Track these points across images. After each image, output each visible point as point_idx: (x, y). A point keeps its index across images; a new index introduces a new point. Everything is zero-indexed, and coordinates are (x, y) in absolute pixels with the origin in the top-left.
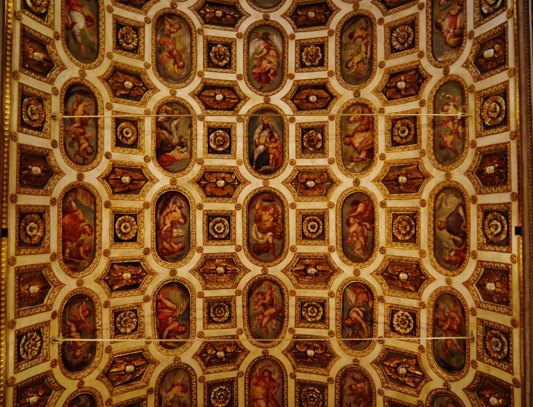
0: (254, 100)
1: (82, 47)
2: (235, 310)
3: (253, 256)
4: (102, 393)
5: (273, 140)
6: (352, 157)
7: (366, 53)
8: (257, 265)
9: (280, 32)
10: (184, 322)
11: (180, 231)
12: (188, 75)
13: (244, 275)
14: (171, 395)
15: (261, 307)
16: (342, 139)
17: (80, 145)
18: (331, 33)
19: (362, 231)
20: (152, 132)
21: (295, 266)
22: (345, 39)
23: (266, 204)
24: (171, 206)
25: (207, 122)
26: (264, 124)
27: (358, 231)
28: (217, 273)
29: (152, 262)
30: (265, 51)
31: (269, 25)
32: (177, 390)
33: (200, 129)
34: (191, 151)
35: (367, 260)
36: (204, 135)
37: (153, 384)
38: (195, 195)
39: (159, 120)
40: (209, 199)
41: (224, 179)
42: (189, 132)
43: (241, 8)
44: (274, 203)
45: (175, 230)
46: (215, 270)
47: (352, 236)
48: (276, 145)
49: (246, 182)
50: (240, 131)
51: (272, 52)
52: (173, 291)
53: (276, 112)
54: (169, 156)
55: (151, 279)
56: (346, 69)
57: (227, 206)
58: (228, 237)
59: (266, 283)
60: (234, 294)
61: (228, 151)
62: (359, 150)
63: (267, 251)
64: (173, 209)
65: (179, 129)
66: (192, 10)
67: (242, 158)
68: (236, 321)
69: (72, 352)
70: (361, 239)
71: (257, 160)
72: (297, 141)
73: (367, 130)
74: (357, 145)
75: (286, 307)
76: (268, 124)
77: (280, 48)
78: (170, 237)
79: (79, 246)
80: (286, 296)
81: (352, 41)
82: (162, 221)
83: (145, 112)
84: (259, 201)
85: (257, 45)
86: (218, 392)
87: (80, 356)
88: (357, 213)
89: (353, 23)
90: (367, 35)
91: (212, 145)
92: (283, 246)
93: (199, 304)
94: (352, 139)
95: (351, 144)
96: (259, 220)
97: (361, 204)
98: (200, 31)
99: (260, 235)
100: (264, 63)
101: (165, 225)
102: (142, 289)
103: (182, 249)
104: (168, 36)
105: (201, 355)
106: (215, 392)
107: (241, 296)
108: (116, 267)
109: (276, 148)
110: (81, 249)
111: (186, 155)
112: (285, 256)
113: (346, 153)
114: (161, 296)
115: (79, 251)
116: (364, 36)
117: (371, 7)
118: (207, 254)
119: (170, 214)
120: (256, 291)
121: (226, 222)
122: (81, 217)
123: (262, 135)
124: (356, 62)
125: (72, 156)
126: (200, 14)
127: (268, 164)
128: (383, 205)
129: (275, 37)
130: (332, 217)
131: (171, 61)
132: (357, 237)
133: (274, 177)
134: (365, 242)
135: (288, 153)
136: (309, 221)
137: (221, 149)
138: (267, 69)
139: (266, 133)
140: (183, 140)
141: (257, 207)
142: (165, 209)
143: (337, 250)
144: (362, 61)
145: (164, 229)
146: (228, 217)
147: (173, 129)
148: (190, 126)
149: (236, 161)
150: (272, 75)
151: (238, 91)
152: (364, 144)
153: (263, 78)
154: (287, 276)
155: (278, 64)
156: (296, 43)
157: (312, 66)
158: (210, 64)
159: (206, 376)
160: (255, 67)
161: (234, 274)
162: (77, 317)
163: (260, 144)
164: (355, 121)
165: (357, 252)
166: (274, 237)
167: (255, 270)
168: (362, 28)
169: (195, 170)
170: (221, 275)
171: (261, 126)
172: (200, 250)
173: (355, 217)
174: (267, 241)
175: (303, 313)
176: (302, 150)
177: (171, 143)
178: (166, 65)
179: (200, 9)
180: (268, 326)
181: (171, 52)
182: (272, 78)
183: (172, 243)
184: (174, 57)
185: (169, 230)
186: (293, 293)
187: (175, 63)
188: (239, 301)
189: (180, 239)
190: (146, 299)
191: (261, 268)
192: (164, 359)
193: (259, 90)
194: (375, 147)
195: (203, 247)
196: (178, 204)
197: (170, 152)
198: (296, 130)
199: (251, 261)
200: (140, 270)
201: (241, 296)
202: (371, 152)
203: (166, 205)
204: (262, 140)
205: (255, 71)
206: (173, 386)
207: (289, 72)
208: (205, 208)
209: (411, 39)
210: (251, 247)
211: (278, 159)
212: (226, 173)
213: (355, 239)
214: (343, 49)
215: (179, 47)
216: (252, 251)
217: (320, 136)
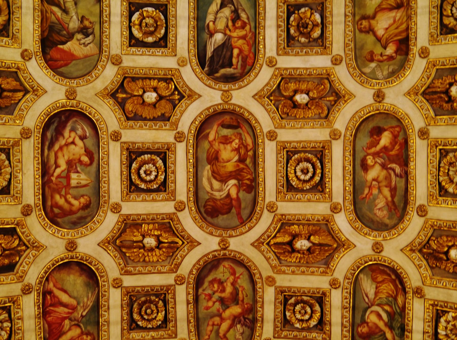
2: (175, 308)
3: (204, 219)
5: (239, 24)
6: (372, 53)
8: (211, 234)
10: (89, 328)
11: (83, 176)
13: (189, 251)
15: (217, 304)
16: (355, 23)
19: (388, 178)
20: (34, 9)
21: (275, 237)
23: (226, 132)
24: (66, 133)
27: (381, 178)
28: (144, 247)
29: (37, 228)
35: (395, 226)
36: (122, 15)
38: (108, 116)
40: (131, 123)
41: (155, 90)
42: (96, 9)
44: (240, 130)
45: (74, 176)
46: (141, 241)
47: (370, 187)
48: (242, 33)
49: (193, 96)
52: (72, 277)
54: (63, 51)
55: (35, 257)
58: (163, 187)
59: (226, 264)
60: (173, 282)
61: (163, 43)
63: (228, 211)
64: (71, 140)
67: (186, 55)
68: (175, 326)
70: (386, 192)
71: (212, 57)
72: (279, 26)
73: (398, 7)
74: (380, 32)
75: (259, 305)
80: (259, 285)
84: (215, 127)
88: (378, 148)
91: (136, 33)
92: (255, 202)
93: (115, 298)
94: (373, 22)
95: (371, 30)
96: (214, 159)
99: (216, 184)
101: (57, 166)
102: (20, 273)
103: (86, 207)
107: (184, 286)
109: (244, 37)
111: (92, 49)
112: (258, 220)
113: (362, 48)
114: (51, 285)
118: (128, 216)
119: (65, 149)
120: (210, 278)
121: (160, 163)
123: (219, 15)
127: (230, 65)
128: (423, 134)
130: (338, 154)
132: (379, 188)
133: (240, 88)
134: (393, 196)
136: (299, 161)
137: (150, 39)
139: (227, 12)
140: (87, 23)
141: (211, 137)
142: (57, 139)
146: (163, 153)
149: (175, 59)
152: (392, 31)
154: (262, 252)
161: (173, 248)
163: (217, 31)
165: (379, 213)
166: (239, 187)
167: (208, 243)
169: (108, 75)
170: (151, 250)
172: (116, 208)
174: (228, 195)
175: (288, 314)
176: (288, 42)
177: (67, 29)
180: (228, 335)
183: (69, 196)
185: (64, 174)
186: (271, 281)
188: (182, 294)
189: (82, 191)
190: (27, 290)
191: (218, 239)
194: (412, 36)
195: (121, 204)
196: (80, 132)
197: (64, 43)
199: (201, 227)
200: (17, 242)
201: (184, 286)
202: (404, 44)
203: (59, 133)
204: (221, 25)
208: (123, 139)
211: (247, 56)
212: (160, 80)
213: (375, 191)
216: (202, 210)
217: (317, 17)
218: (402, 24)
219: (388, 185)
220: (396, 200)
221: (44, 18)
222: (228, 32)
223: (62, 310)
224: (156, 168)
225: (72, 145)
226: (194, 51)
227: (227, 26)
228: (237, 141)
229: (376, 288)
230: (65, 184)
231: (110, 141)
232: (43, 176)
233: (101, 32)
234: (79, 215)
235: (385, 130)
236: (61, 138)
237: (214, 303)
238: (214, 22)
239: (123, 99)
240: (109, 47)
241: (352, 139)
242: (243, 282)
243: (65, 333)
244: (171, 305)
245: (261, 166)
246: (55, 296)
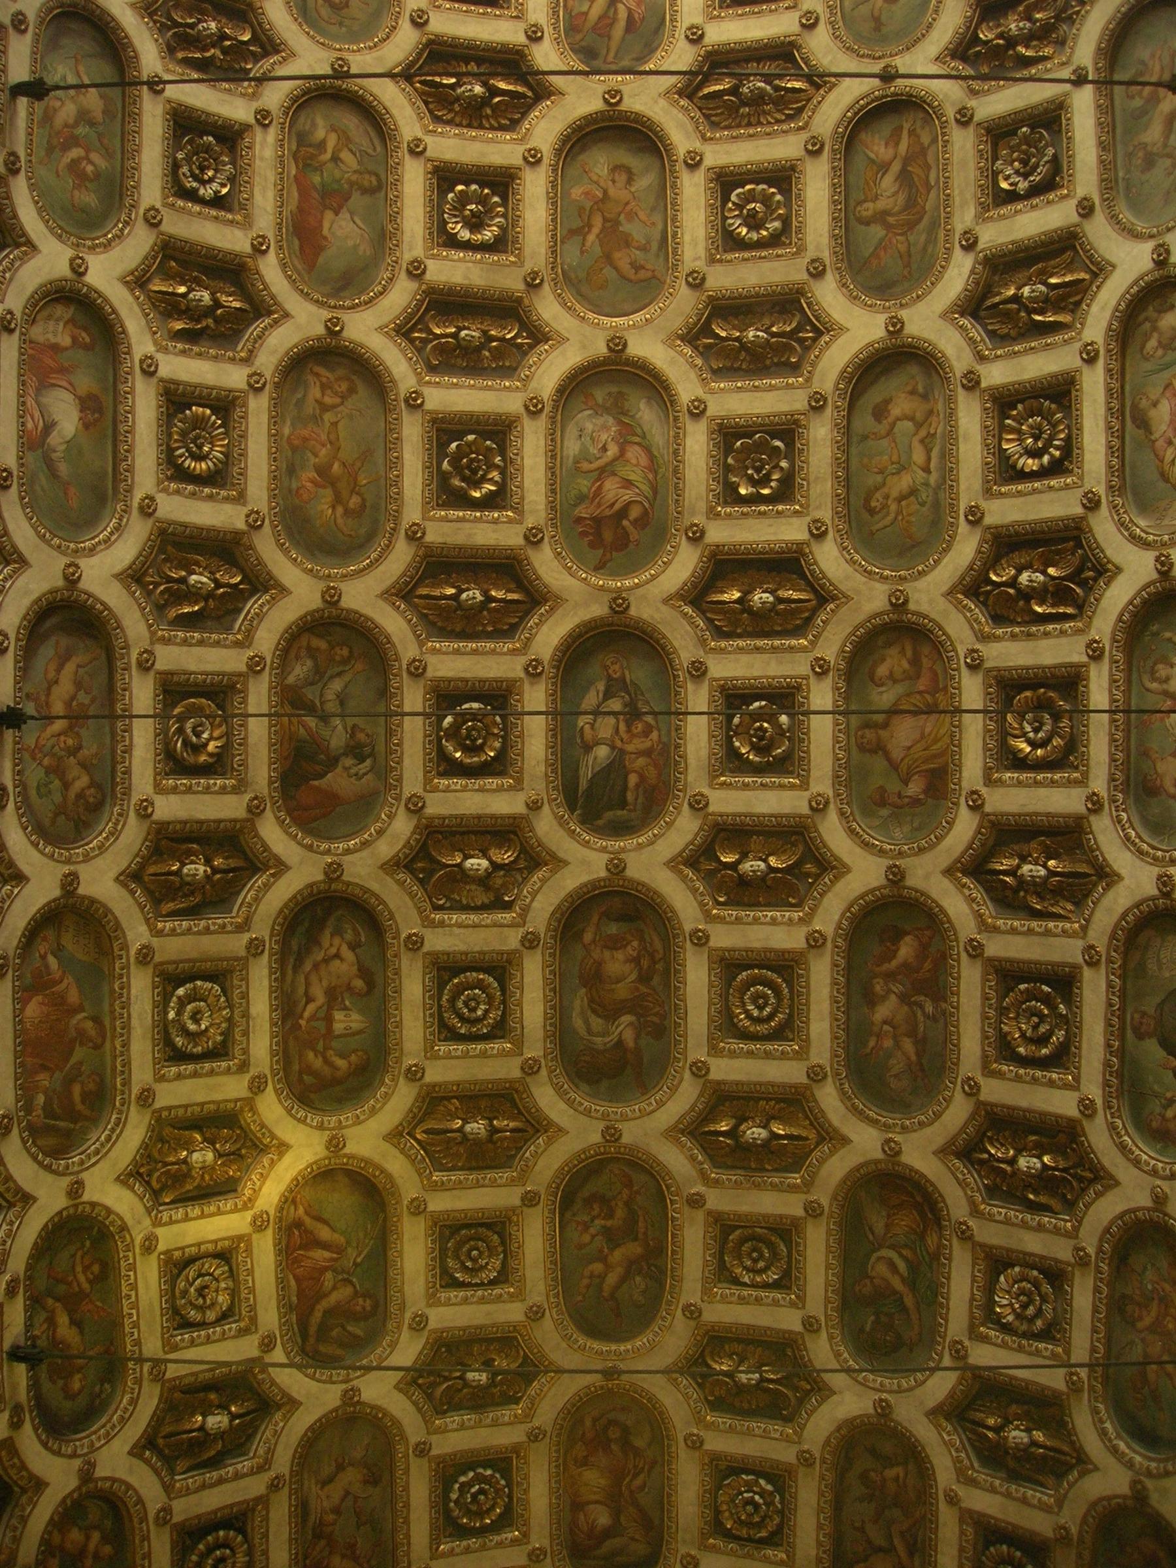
1: (72, 490)
4: (142, 1491)
5: (639, 727)
7: (927, 470)
11: (355, 1016)
14: (335, 1492)
17: (66, 786)
23: (613, 929)
24: (326, 942)
26: (610, 678)
32: (351, 1477)
37: (283, 1462)
38: (400, 902)
39: (291, 680)
45: (338, 1015)
47: (879, 1036)
54: (318, 789)
56: (866, 516)
58: (500, 1030)
60: (518, 1202)
64: (333, 951)
69: (61, 1383)
70: (908, 1045)
71: (590, 788)
74: (897, 754)
79: (69, 1082)
82: (301, 990)
84: (595, 918)
86: (469, 1484)
87: (80, 1391)
94: (883, 734)
95: (879, 748)
96: (594, 978)
97: (908, 939)
99: (597, 1023)
101: (309, 1000)
105: (417, 1380)
106: (462, 1485)
108: (167, 1131)
109: (648, 753)
110: (77, 1090)
116: (919, 416)
119: (323, 966)
124: (894, 493)
126: (412, 341)
127: (623, 804)
129: (642, 405)
131: (327, 494)
132: (895, 1037)
138: (617, 506)
140: (361, 736)
141: (588, 937)
142: (308, 951)
144: (913, 492)
146: (500, 969)
147: (332, 707)
150: (635, 523)
153: (608, 535)
155: (655, 493)
159: (434, 1439)
162: (70, 1284)
164: (892, 678)
168: (913, 392)
171: (601, 686)
173: (890, 976)
174: (620, 1043)
179: (413, 329)
182: (634, 534)
184: (332, 483)
185: (322, 1014)
187: (338, 500)
192: (313, 1395)
196: (349, 935)
197: (321, 776)
202: (939, 779)
203: (312, 940)
205: (583, 511)
206: (340, 1468)
213: (888, 1043)
214: (854, 451)
219: (912, 1033)
223: (320, 1255)
228: (635, 944)
229: (889, 1216)
230: (323, 1031)
235: (907, 933)
237: (593, 1237)
243: (326, 1295)
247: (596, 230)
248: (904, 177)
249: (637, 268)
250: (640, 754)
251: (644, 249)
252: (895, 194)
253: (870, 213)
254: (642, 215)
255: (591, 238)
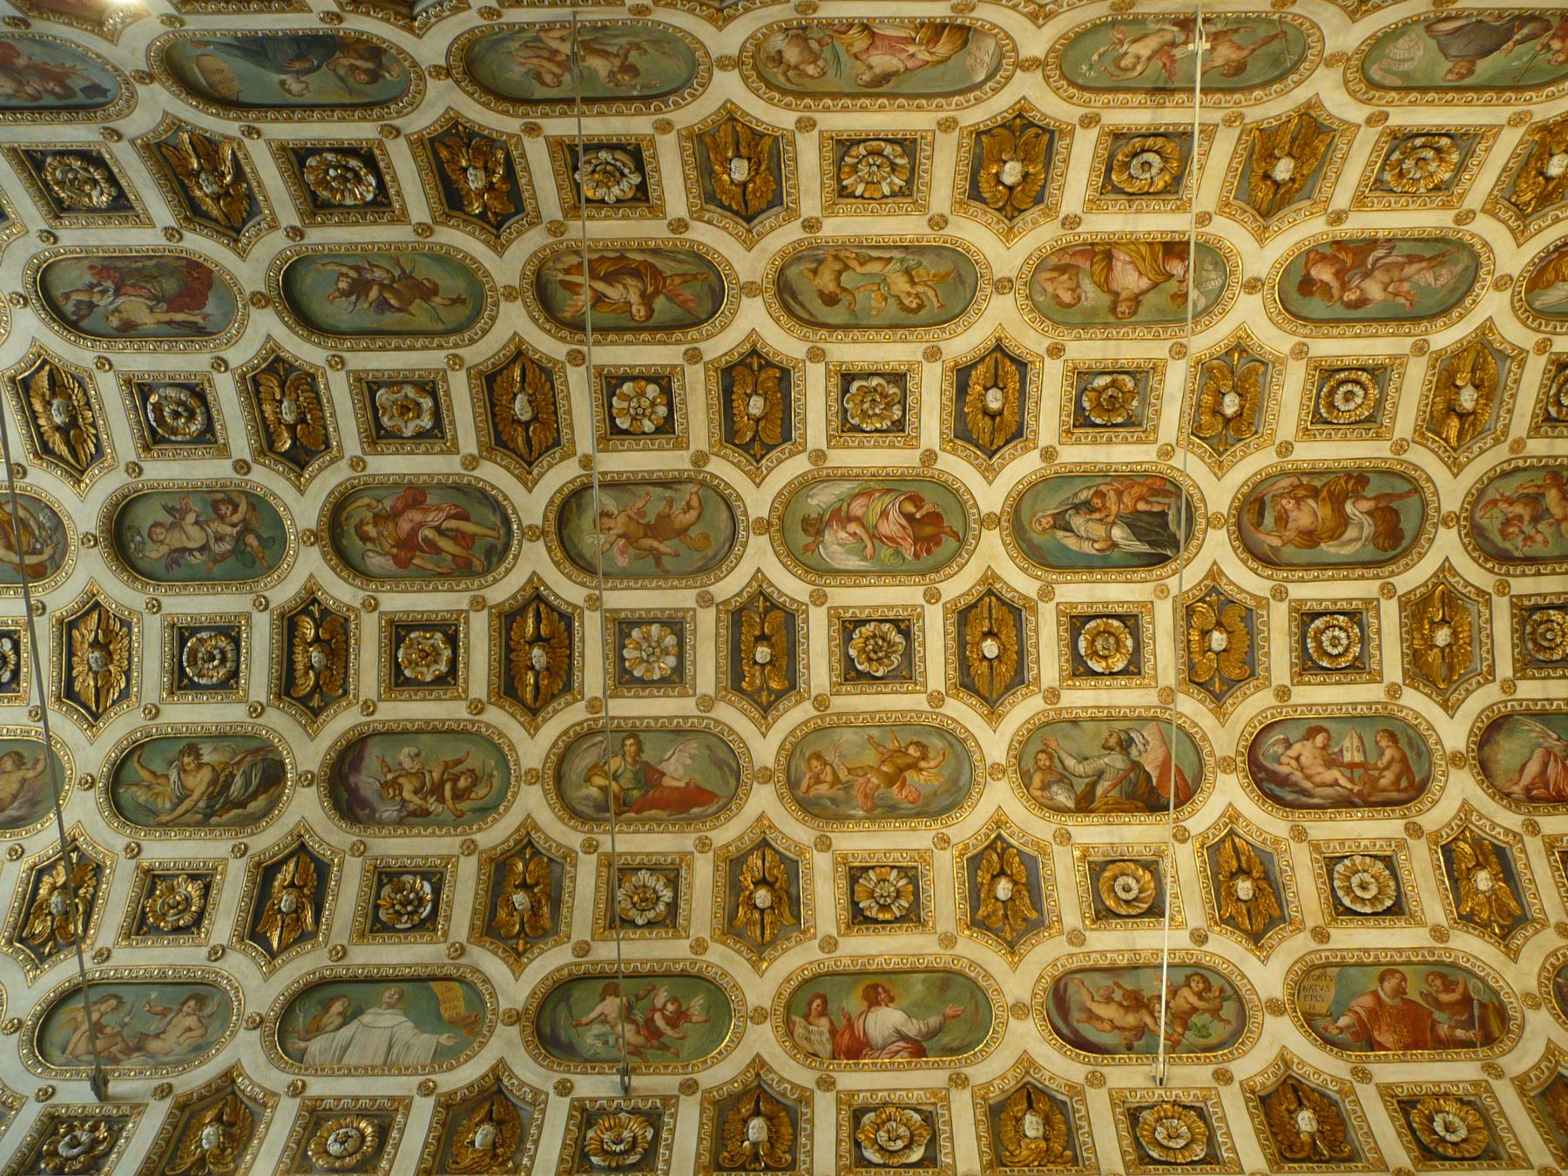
0: (993, 557)
1: (949, 1011)
2: (1545, 596)
3: (1406, 552)
5: (1097, 502)
6: (1175, 297)
8: (1431, 541)
9: (802, 486)
11: (1347, 743)
12: (941, 732)
13: (1456, 574)
15: (1540, 527)
16: (1119, 325)
18: (816, 355)
19: (1387, 268)
20: (1110, 824)
21: (1446, 440)
22: (836, 315)
23: (1269, 520)
24: (1284, 770)
25: (1062, 679)
26: (1054, 527)
27: (1386, 279)
28: (1449, 645)
29: (1438, 814)
30: (853, 527)
31: (781, 519)
33: (1082, 698)
34: (1140, 718)
35: (1475, 257)
36: (1095, 688)
39: (1071, 804)
40: (1260, 670)
41: (1205, 633)
43: (739, 594)
44: (1267, 499)
45: (1347, 757)
46: (1442, 650)
48: (1112, 496)
49: (1215, 573)
50: (1079, 592)
51: (857, 508)
53: (1022, 496)
55: (1481, 816)
56: (923, 312)
57: (1279, 621)
59: (1478, 514)
61: (1131, 621)
62: (1160, 278)
63: (1395, 513)
64: (1293, 763)
65: (1086, 752)
66: (768, 728)
67: (1151, 585)
70: (1410, 270)
71: (1150, 543)
72: (1109, 441)
73: (1108, 257)
74: (1144, 283)
75: (1551, 462)
76: (1054, 516)
77: (845, 488)
78: (1366, 770)
79: (1439, 1005)
80: (1521, 463)
81: (846, 298)
82: (1329, 791)
83: (1068, 846)
84: (1261, 536)
85: (837, 547)
88: (1334, 284)
89: (794, 296)
90: (836, 257)
91: (1119, 664)
92: (1389, 473)
93: (1529, 690)
94: (1123, 296)
95: (1136, 300)
96: (1310, 538)
97: (1313, 272)
98: (821, 703)
99: (1351, 533)
100: (886, 528)
101: (1336, 783)
102: (1510, 839)
103: (1392, 736)
104: (847, 787)
107: (1512, 581)
109: (1119, 494)
111: (1150, 732)
112: (1416, 468)
113: (1162, 311)
114: (1516, 789)
115: (1451, 1005)
117: (763, 251)
118: (1405, 672)
120: (1498, 539)
121: (1319, 623)
122: (1367, 1001)
123: (1083, 534)
124: (907, 288)
125: (1229, 1028)
127: (1163, 514)
128: (1338, 218)
129: (812, 502)
131: (911, 776)
133: (1203, 500)
134: (1421, 259)
135: (1140, 463)
136: (1331, 406)
137: (1129, 643)
138: (903, 522)
139: (1077, 521)
140: (1112, 741)
141: (1276, 542)
142: (1295, 784)
143: (1426, 332)
144: (907, 272)
145: (1349, 786)
146: (1305, 617)
148: (1075, 722)
149: (1158, 603)
150: (919, 508)
151: (971, 599)
152: (1146, 266)
153: (929, 530)
154: (1470, 461)
155: (889, 491)
156: (834, 447)
157: (903, 402)
158: (906, 673)
160: (898, 553)
161: (1451, 600)
163: (1109, 537)
165: (1442, 281)
166: (1358, 497)
167: (1447, 546)
168: (815, 272)
169: (1190, 707)
170: (1455, 634)
171: (1060, 534)
172: (1393, 691)
173: (1344, 287)
174: (1370, 513)
176: (1133, 424)
177: (1127, 772)
178: (925, 791)
181: (890, 780)
182: (927, 508)
183: (1380, 765)
184: (901, 770)
185: (1347, 772)
186: (1519, 444)
187: (913, 766)
188: (1524, 585)
189: (1369, 743)
190: (1534, 829)
193: (961, 541)
195: (1386, 684)
197: (1149, 777)
198: (1078, 442)
199: (1421, 556)
200: (1462, 845)
201: (1512, 581)
203: (1284, 781)
204: (1099, 530)
207: (917, 463)
208: (1287, 682)
209: (888, 150)
210: (1381, 556)
211: (1150, 489)
212: (1190, 626)
213: (1406, 286)
214: (864, 322)
215: (870, 758)
216: (1391, 553)
217: (1101, 381)
218: (1139, 252)
219: (1401, 266)
220: (1428, 255)
221: (1117, 807)
222: (1111, 519)
223: (1551, 772)
224: (1327, 628)
225: (1299, 758)
226: (1142, 574)
227: (1101, 520)
228: (1284, 502)
230: (1361, 771)
231: (1291, 702)
232: (1354, 805)
233: (1125, 718)
234: (1406, 749)
235: (1308, 273)
236: (1293, 778)
238: (1095, 541)
239: (1222, 683)
240: (1148, 708)
241: (1310, 326)
242: (1510, 487)
244: (1540, 601)
245: (1331, 464)
246: (1533, 783)
247: (655, 544)
248: (609, 279)
249: (689, 507)
250: (1120, 500)
251: (671, 502)
252: (625, 286)
253: (642, 309)
254: (640, 504)
255: (662, 547)
